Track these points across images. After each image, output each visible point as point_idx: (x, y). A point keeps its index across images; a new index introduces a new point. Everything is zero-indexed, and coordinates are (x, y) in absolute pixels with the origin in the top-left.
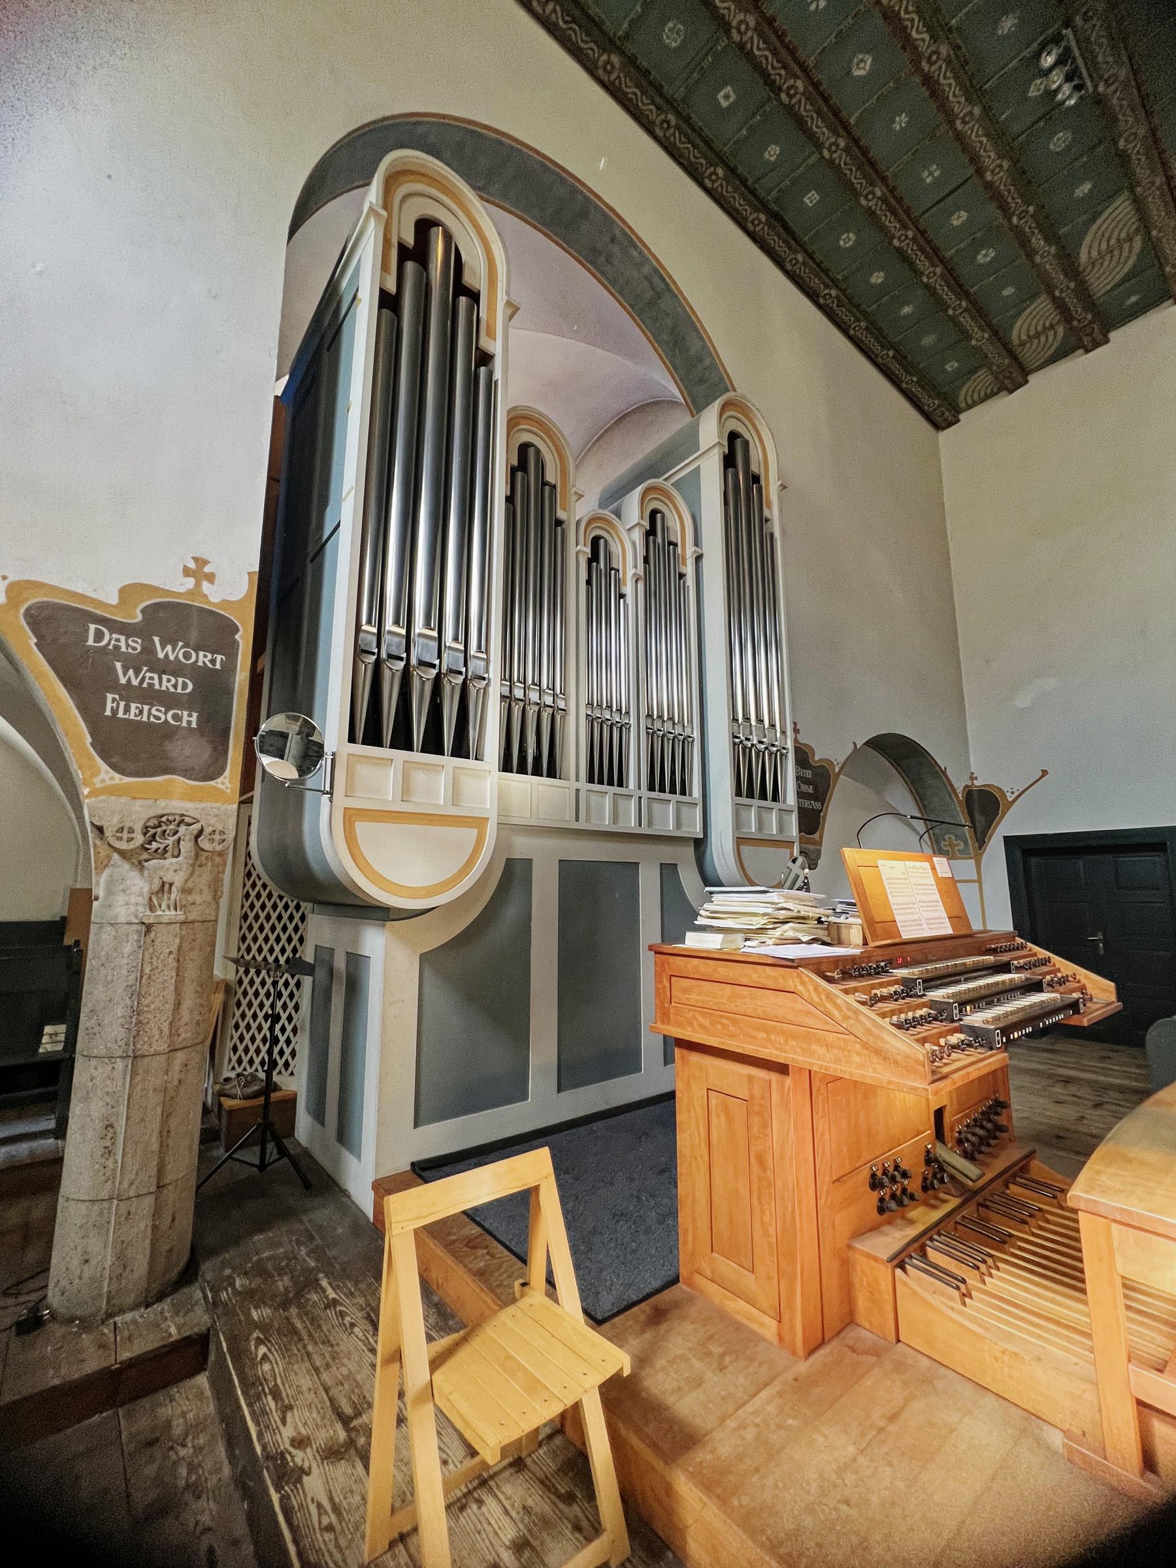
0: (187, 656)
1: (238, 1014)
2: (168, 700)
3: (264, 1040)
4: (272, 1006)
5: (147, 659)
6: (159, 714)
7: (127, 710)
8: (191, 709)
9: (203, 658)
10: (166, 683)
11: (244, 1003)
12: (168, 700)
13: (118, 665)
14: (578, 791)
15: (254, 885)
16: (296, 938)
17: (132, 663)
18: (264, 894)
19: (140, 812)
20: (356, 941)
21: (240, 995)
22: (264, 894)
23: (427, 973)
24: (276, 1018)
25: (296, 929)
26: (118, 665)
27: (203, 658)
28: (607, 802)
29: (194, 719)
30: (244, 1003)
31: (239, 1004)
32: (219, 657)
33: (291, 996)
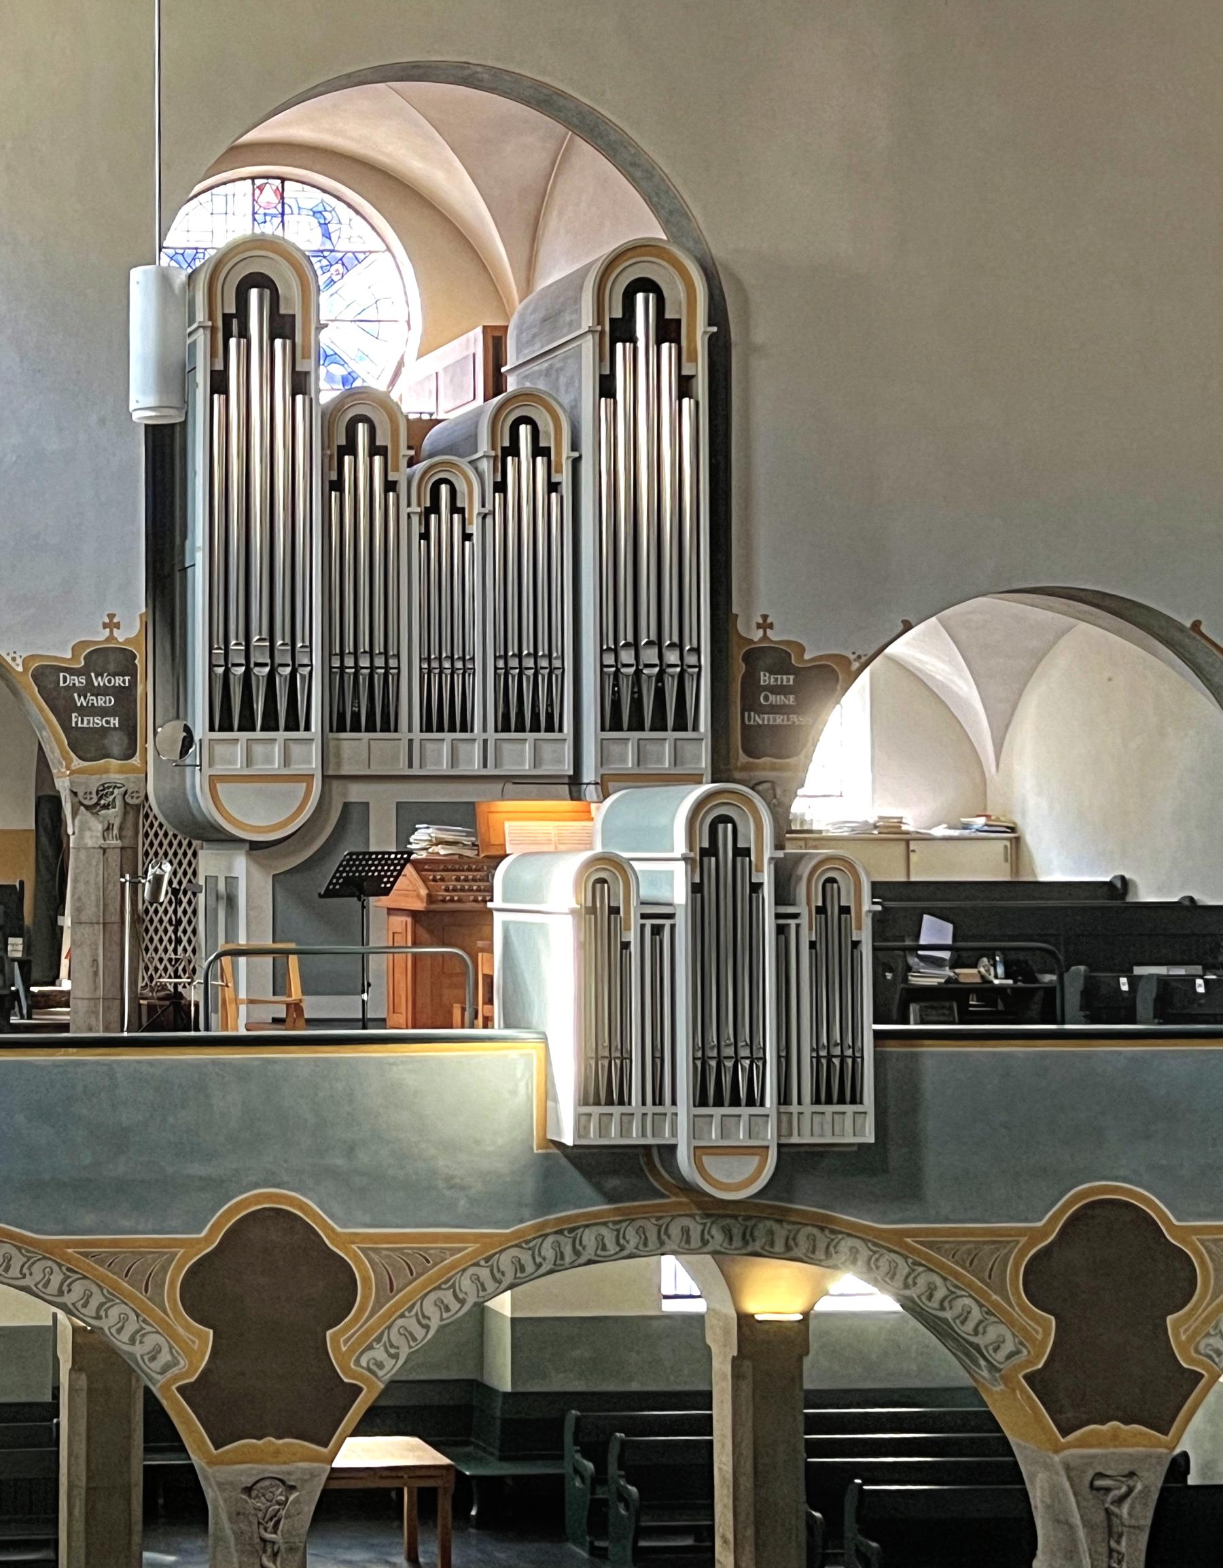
0: (109, 681)
1: (147, 938)
2: (103, 712)
3: (170, 941)
4: (175, 912)
5: (89, 689)
6: (98, 722)
7: (82, 722)
8: (114, 716)
9: (118, 681)
10: (100, 702)
11: (151, 929)
12: (103, 712)
13: (76, 695)
14: (411, 741)
15: (151, 826)
16: (190, 872)
17: (83, 693)
18: (161, 833)
19: (94, 783)
20: (230, 867)
21: (147, 923)
22: (161, 833)
23: (278, 889)
24: (179, 922)
25: (190, 864)
26: (76, 695)
27: (118, 681)
28: (446, 749)
29: (117, 722)
30: (151, 929)
31: (147, 930)
32: (127, 678)
33: (190, 922)
